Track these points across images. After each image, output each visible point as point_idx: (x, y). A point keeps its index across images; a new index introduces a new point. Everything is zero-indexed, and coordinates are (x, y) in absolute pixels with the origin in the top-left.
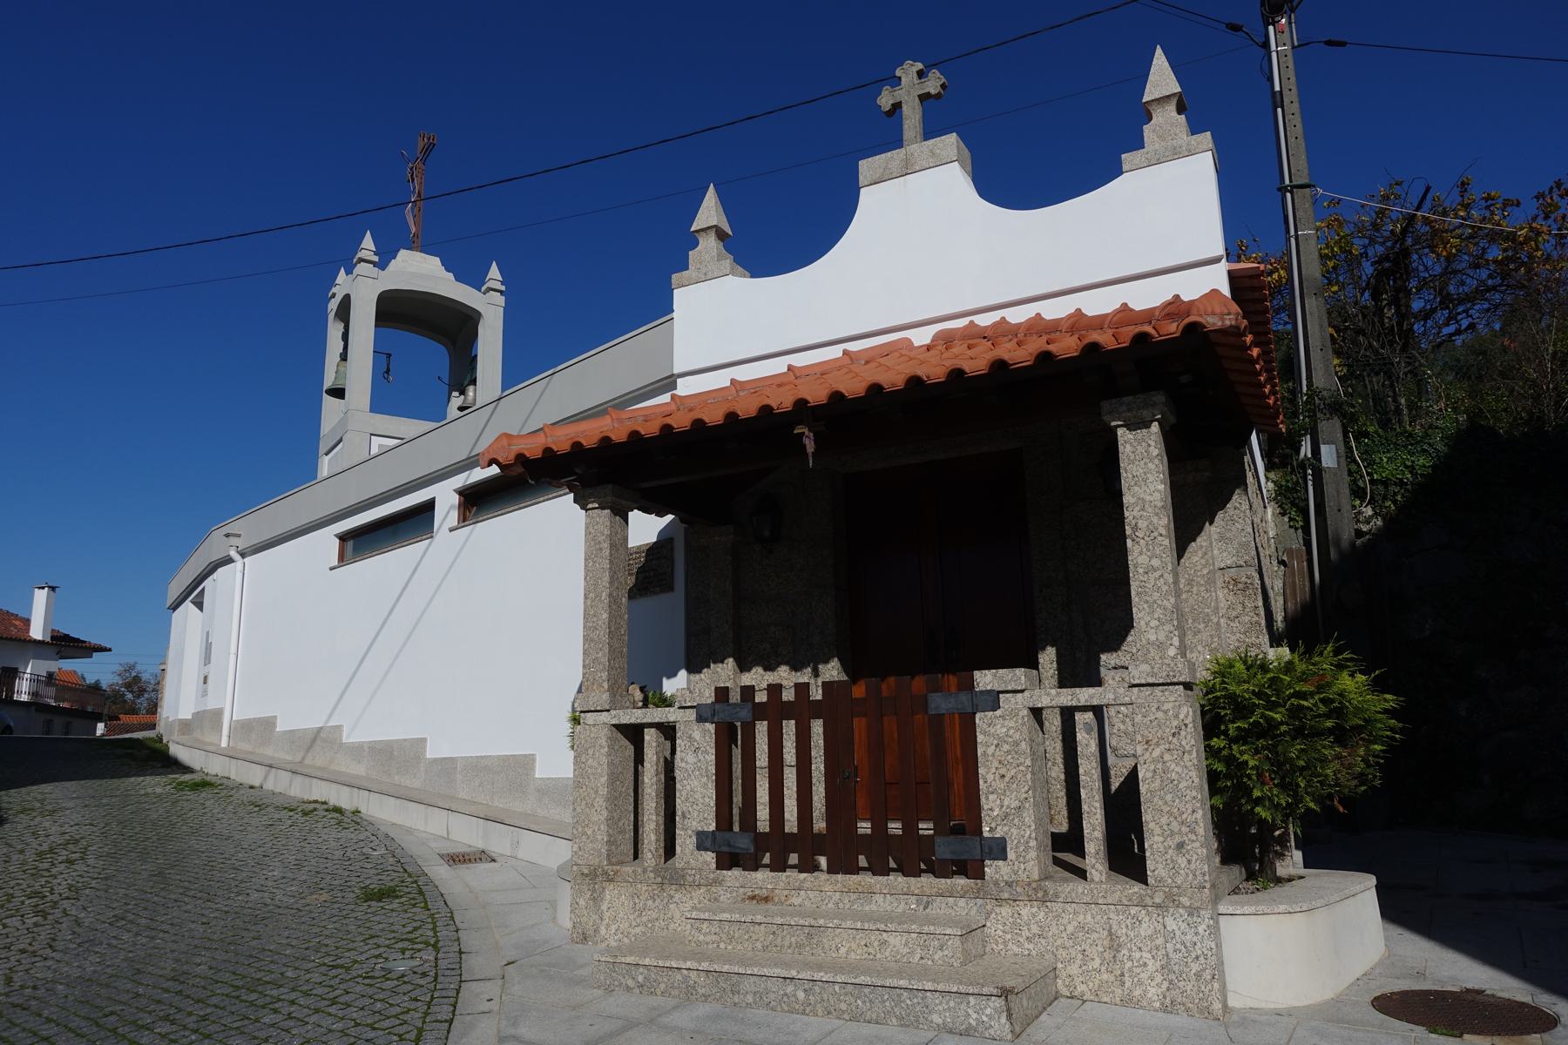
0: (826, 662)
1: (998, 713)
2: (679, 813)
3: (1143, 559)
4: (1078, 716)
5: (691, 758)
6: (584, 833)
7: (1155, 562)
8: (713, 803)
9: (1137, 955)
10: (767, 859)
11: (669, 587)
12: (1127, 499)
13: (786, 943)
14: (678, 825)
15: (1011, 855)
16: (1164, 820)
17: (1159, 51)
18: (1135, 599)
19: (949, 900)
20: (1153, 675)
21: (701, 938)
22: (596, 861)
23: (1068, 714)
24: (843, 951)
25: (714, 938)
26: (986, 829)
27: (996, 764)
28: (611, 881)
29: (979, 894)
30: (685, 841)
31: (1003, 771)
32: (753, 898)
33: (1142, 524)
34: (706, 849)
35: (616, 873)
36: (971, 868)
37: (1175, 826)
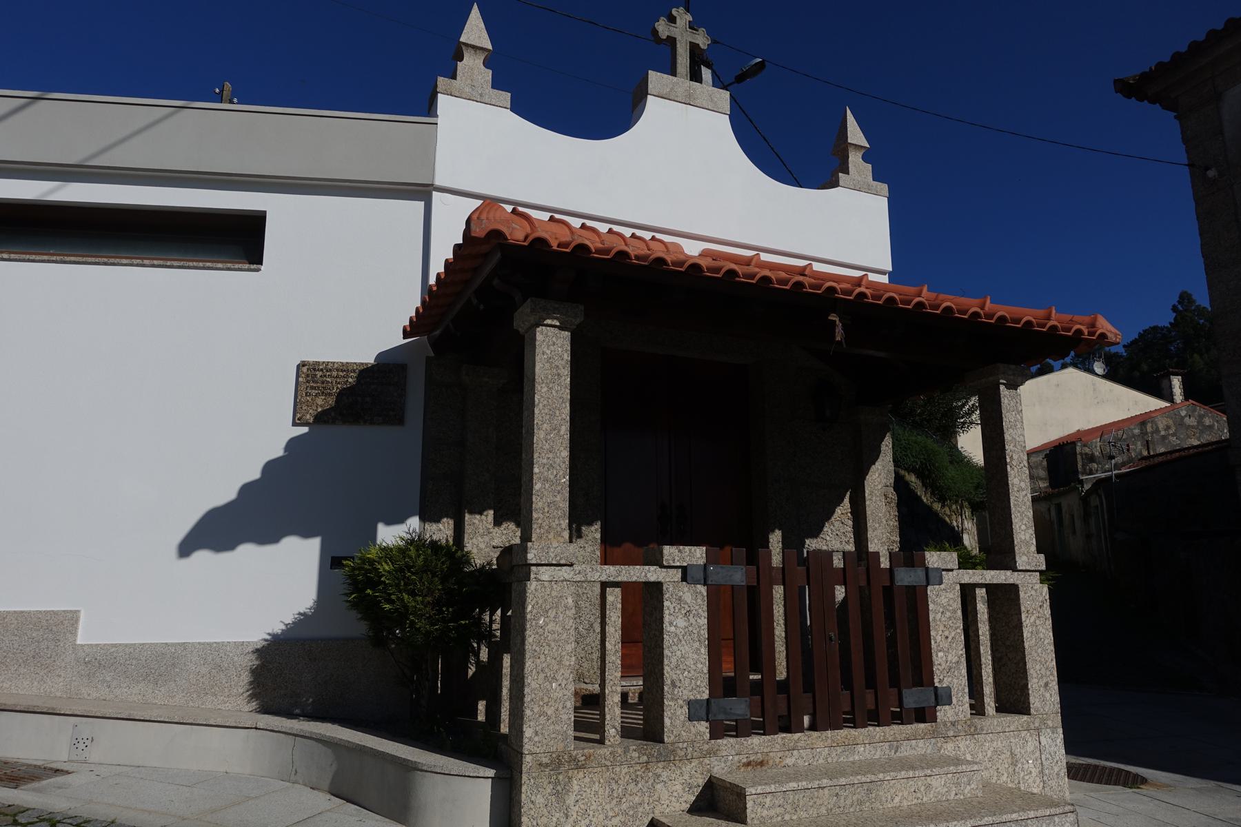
0: (590, 524)
1: (942, 586)
2: (668, 682)
3: (1016, 481)
4: (978, 591)
5: (681, 623)
6: (545, 714)
7: (1023, 484)
8: (706, 670)
9: (1026, 766)
10: (806, 720)
11: (397, 418)
12: (1007, 437)
13: (849, 802)
14: (667, 696)
15: (954, 700)
16: (1038, 667)
17: (475, 6)
18: (1013, 509)
19: (909, 741)
20: (1029, 564)
21: (765, 813)
22: (561, 746)
23: (967, 592)
24: (897, 800)
25: (778, 810)
26: (936, 681)
27: (942, 628)
28: (583, 767)
29: (935, 735)
30: (674, 715)
31: (946, 633)
32: (748, 764)
33: (1015, 457)
34: (699, 720)
35: (588, 758)
36: (924, 715)
37: (1043, 671)
